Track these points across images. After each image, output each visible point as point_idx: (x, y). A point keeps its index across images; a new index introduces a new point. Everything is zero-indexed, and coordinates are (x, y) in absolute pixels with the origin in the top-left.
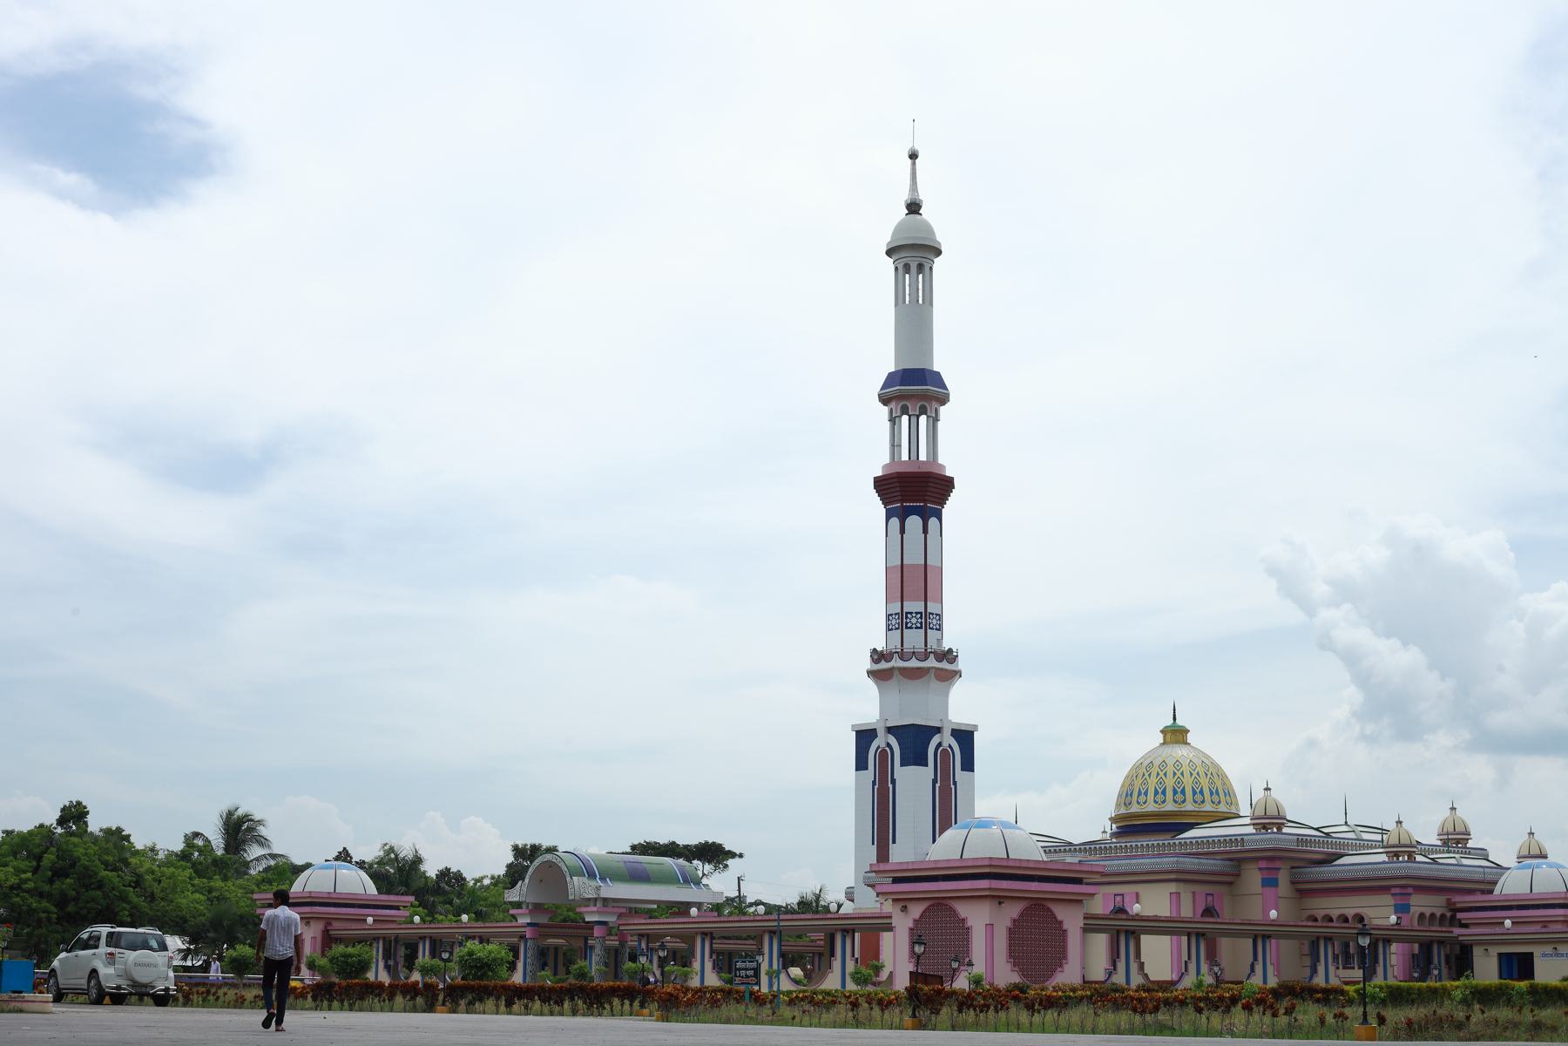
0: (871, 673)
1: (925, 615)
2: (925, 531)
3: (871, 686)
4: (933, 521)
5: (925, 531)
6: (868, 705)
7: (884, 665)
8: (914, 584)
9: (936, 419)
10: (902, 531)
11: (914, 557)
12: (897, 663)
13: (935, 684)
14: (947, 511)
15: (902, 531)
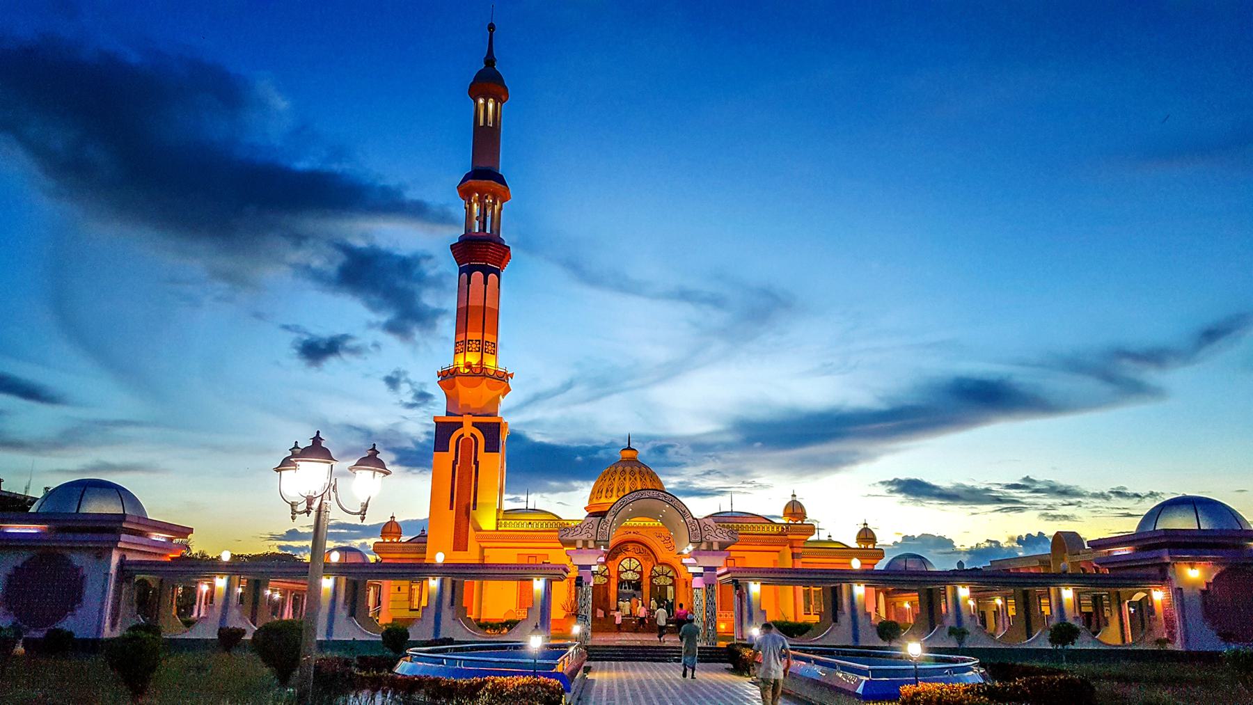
2: (486, 282)
5: (486, 282)
11: (476, 301)
15: (469, 282)
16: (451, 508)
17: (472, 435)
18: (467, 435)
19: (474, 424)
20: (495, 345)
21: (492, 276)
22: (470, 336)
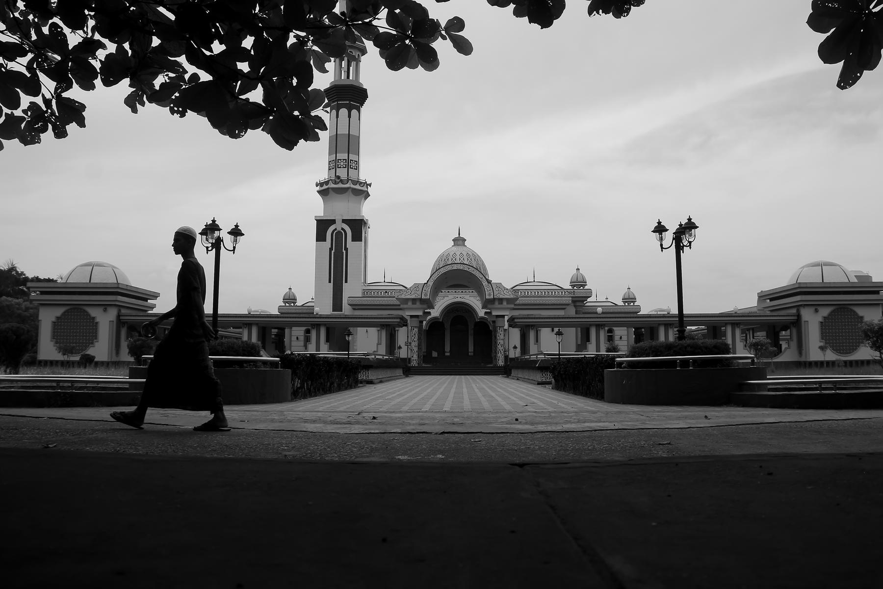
0: (318, 192)
1: (348, 161)
2: (349, 116)
3: (319, 198)
4: (354, 112)
5: (349, 116)
6: (317, 207)
7: (325, 187)
8: (343, 143)
9: (358, 61)
10: (337, 117)
11: (343, 130)
12: (331, 185)
13: (353, 198)
14: (362, 109)
15: (337, 117)
16: (330, 282)
17: (343, 229)
18: (339, 229)
19: (344, 221)
20: (357, 162)
21: (354, 112)
22: (340, 156)
